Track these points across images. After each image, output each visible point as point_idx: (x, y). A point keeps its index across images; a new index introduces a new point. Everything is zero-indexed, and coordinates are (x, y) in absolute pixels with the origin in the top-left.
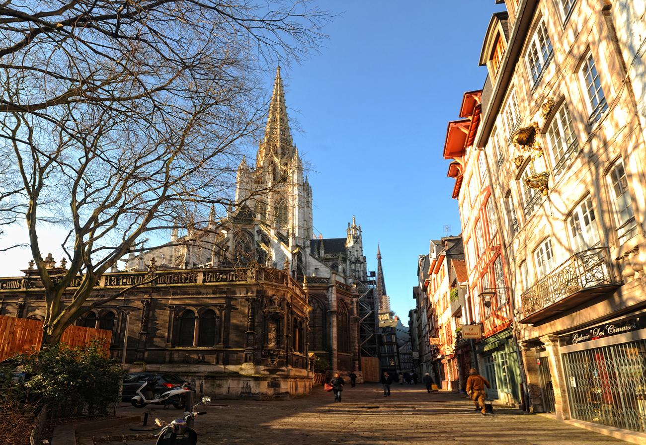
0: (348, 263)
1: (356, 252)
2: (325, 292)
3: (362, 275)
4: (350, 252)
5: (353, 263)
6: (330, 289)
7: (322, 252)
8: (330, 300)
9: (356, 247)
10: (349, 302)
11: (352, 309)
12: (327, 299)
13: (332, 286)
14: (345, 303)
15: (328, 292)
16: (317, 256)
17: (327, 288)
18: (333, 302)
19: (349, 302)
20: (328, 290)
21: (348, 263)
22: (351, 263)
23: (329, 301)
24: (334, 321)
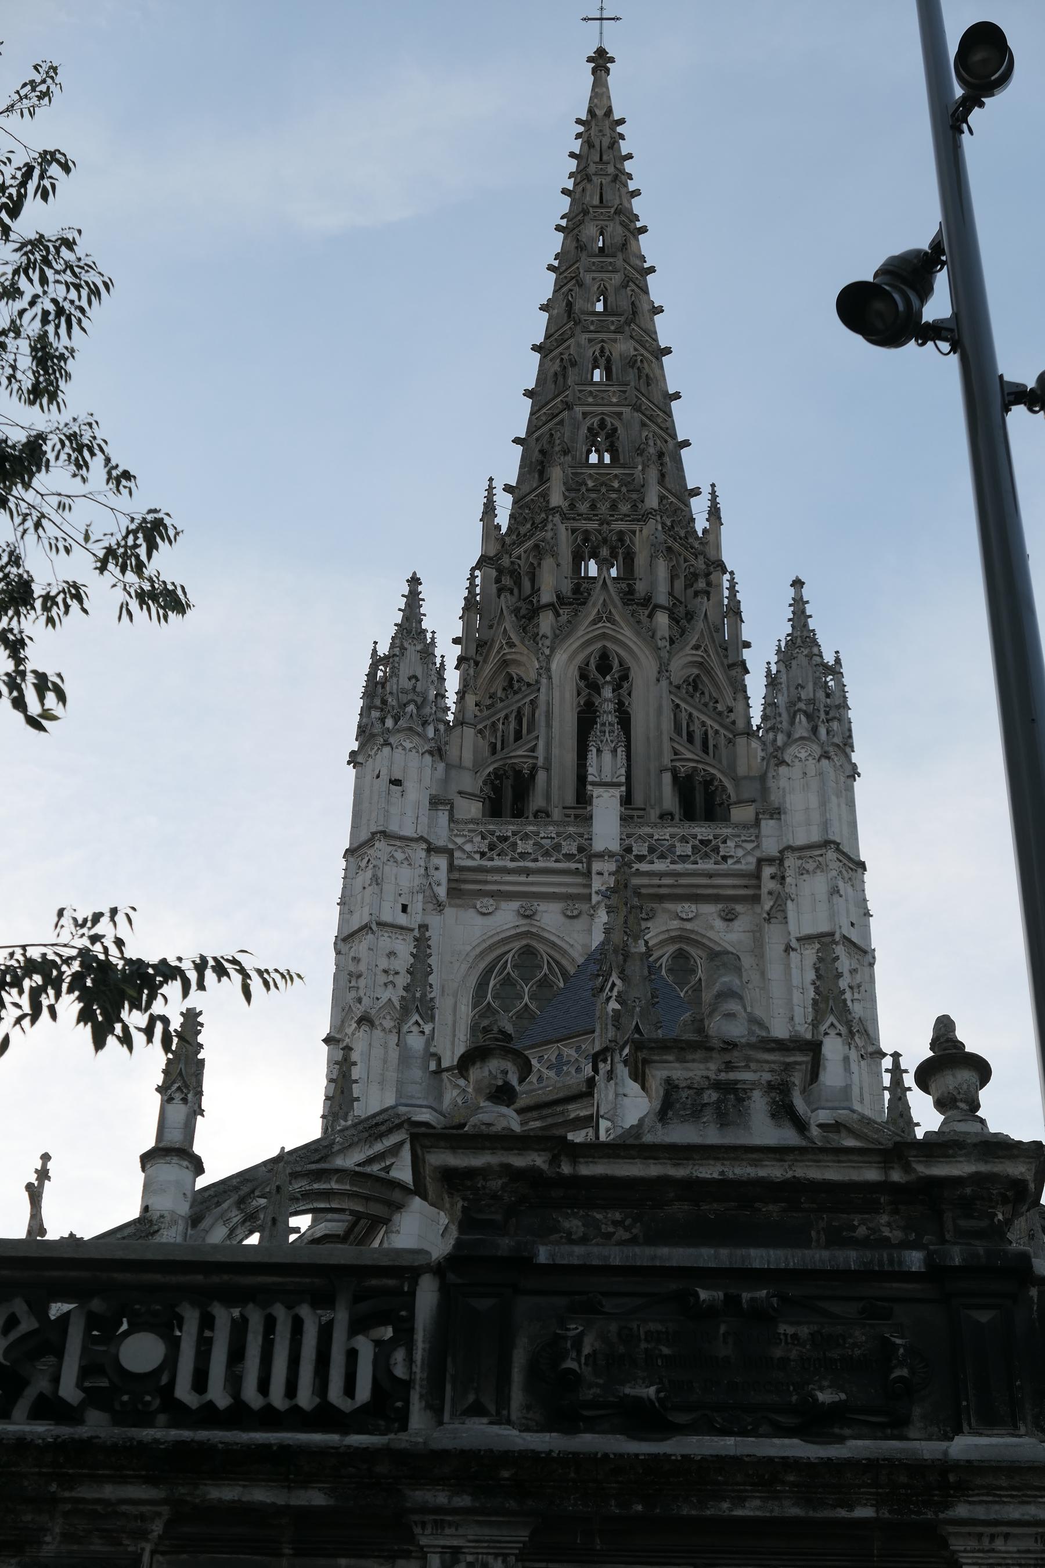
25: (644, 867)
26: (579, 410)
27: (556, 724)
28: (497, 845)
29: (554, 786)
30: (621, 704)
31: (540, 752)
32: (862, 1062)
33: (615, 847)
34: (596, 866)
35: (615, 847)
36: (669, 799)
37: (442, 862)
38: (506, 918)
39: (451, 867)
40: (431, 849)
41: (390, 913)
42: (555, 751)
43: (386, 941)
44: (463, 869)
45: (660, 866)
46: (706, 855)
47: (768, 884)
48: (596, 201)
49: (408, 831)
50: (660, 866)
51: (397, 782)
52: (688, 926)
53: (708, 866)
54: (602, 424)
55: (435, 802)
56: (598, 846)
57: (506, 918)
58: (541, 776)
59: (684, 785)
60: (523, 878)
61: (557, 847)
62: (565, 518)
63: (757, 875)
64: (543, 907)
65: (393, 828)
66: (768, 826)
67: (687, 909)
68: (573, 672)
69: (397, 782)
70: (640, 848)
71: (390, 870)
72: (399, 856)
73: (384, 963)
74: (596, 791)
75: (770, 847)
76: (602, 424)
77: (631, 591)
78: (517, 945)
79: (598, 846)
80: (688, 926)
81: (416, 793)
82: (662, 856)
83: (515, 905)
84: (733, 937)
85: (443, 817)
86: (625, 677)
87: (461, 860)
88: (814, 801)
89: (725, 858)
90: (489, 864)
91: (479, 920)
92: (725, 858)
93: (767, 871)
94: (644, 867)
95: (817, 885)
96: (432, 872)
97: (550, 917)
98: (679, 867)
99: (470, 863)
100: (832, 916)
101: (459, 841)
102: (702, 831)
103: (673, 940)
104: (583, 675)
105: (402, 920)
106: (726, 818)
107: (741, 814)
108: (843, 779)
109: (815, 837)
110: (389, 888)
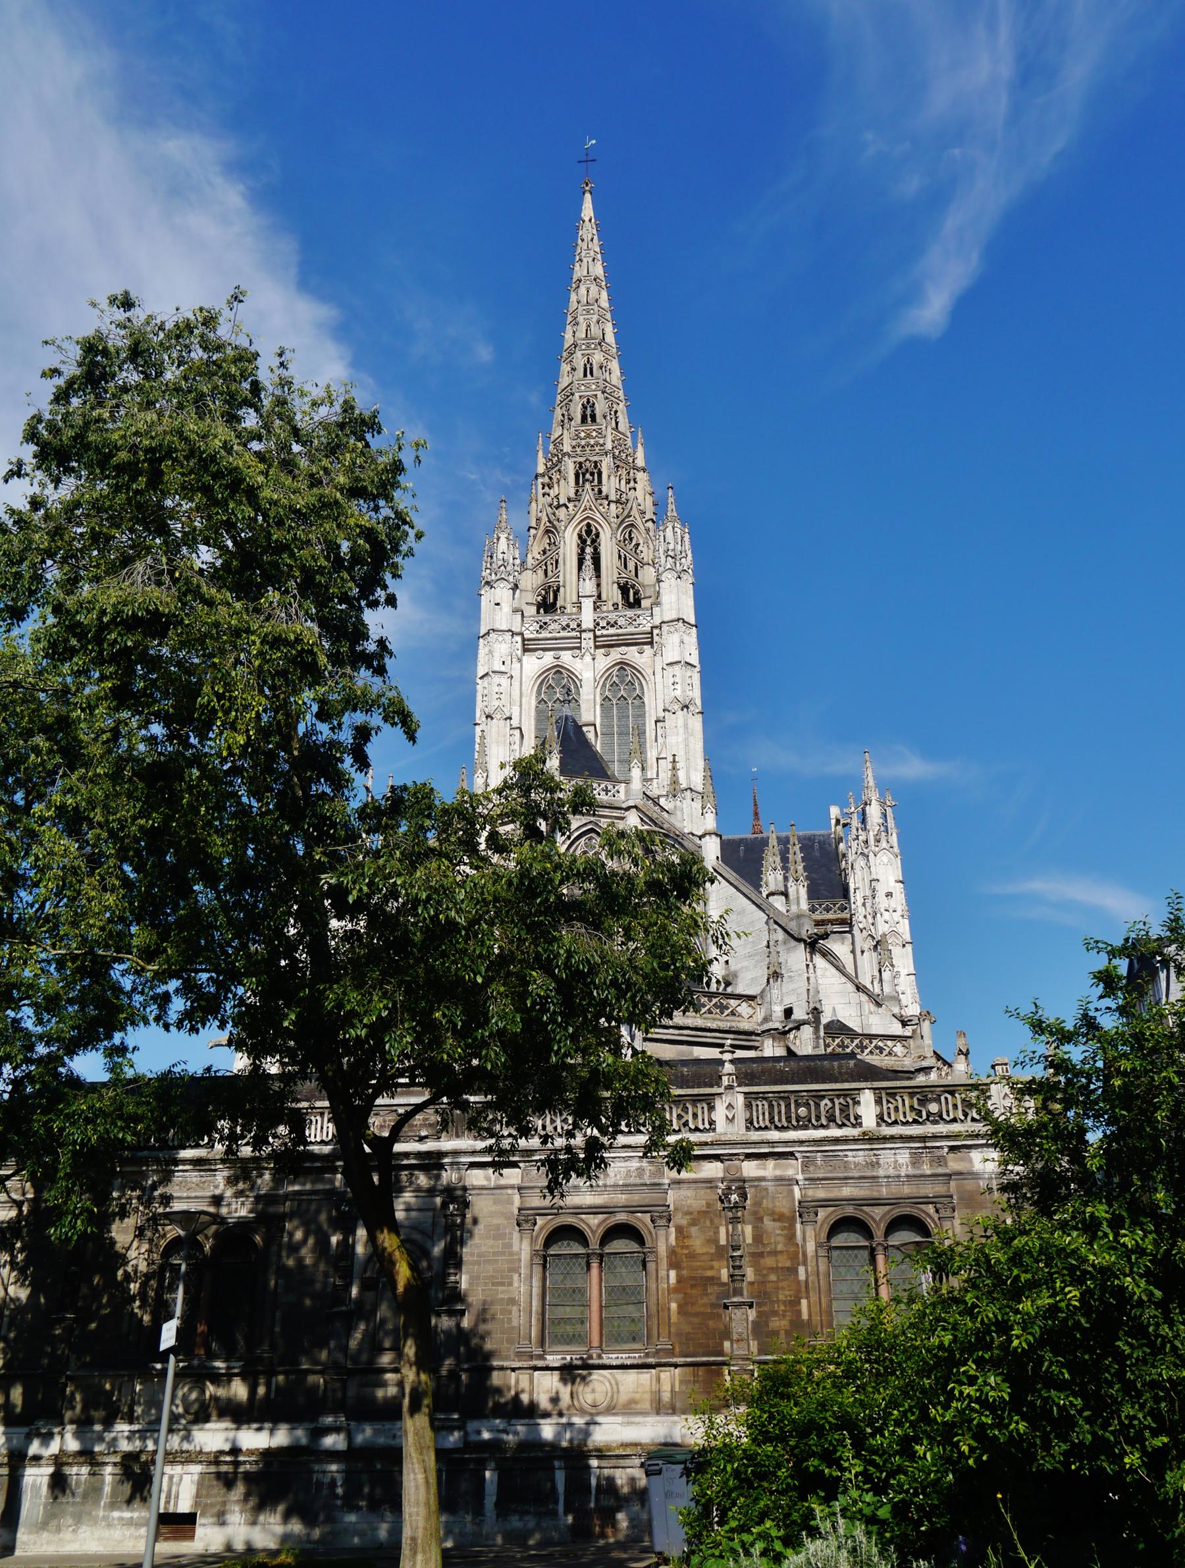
25: (605, 632)
26: (577, 395)
27: (568, 563)
28: (543, 626)
29: (567, 597)
31: (561, 579)
33: (591, 626)
34: (584, 635)
35: (591, 626)
36: (617, 596)
37: (519, 639)
38: (548, 659)
40: (513, 634)
41: (498, 666)
42: (568, 577)
43: (496, 679)
44: (529, 640)
45: (612, 631)
47: (656, 638)
48: (585, 273)
49: (504, 627)
50: (612, 631)
51: (498, 604)
53: (631, 629)
54: (588, 402)
55: (515, 611)
56: (584, 626)
57: (548, 659)
58: (562, 589)
59: (624, 589)
61: (568, 626)
62: (569, 456)
63: (652, 633)
64: (562, 653)
65: (497, 626)
66: (656, 610)
67: (623, 649)
68: (575, 536)
69: (498, 604)
70: (603, 623)
71: (497, 646)
72: (500, 639)
73: (496, 689)
74: (582, 600)
75: (657, 621)
76: (588, 402)
77: (600, 492)
79: (584, 626)
81: (506, 608)
82: (612, 626)
83: (552, 653)
84: (643, 660)
85: (519, 616)
86: (597, 535)
87: (527, 635)
88: (674, 598)
90: (540, 636)
93: (656, 631)
94: (605, 632)
95: (675, 638)
97: (566, 657)
98: (620, 631)
99: (532, 636)
100: (682, 653)
102: (630, 613)
104: (580, 536)
105: (503, 668)
106: (640, 606)
107: (645, 603)
109: (674, 617)
110: (497, 655)
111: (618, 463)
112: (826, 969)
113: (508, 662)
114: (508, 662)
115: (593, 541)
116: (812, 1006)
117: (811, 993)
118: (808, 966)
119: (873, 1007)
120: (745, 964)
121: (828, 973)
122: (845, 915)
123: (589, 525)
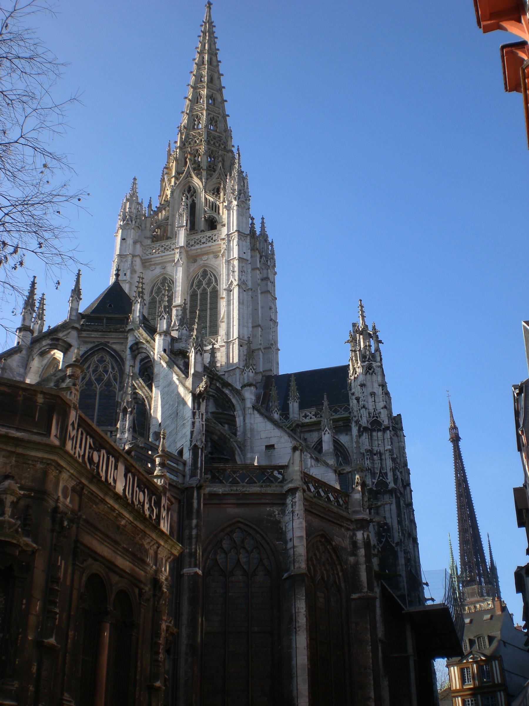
0: (355, 430)
1: (371, 400)
2: (276, 510)
3: (389, 464)
4: (358, 399)
5: (366, 429)
6: (289, 501)
7: (294, 406)
8: (289, 536)
9: (369, 384)
10: (346, 544)
11: (356, 565)
12: (280, 534)
13: (293, 491)
14: (335, 549)
15: (283, 512)
16: (276, 416)
17: (280, 500)
18: (296, 542)
19: (346, 544)
20: (283, 504)
21: (355, 430)
22: (363, 430)
23: (286, 542)
24: (301, 607)
25: (193, 248)
30: (193, 201)
32: (244, 293)
39: (141, 259)
44: (145, 260)
45: (197, 247)
46: (209, 241)
52: (205, 262)
60: (161, 258)
78: (161, 278)
80: (205, 262)
81: (130, 241)
83: (160, 266)
85: (138, 246)
89: (215, 241)
91: (151, 272)
92: (215, 241)
96: (134, 262)
101: (145, 251)
103: (202, 267)
108: (245, 210)
111: (212, 148)
112: (281, 437)
113: (128, 274)
114: (128, 274)
115: (192, 196)
116: (193, 445)
117: (195, 434)
118: (194, 414)
119: (313, 462)
120: (168, 422)
121: (282, 440)
122: (346, 415)
123: (190, 187)
